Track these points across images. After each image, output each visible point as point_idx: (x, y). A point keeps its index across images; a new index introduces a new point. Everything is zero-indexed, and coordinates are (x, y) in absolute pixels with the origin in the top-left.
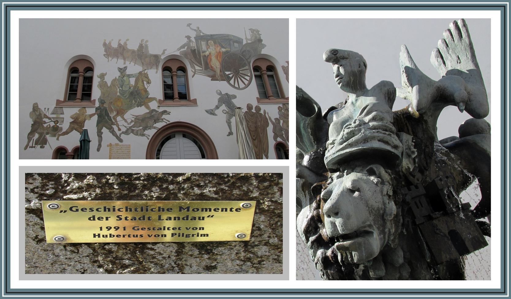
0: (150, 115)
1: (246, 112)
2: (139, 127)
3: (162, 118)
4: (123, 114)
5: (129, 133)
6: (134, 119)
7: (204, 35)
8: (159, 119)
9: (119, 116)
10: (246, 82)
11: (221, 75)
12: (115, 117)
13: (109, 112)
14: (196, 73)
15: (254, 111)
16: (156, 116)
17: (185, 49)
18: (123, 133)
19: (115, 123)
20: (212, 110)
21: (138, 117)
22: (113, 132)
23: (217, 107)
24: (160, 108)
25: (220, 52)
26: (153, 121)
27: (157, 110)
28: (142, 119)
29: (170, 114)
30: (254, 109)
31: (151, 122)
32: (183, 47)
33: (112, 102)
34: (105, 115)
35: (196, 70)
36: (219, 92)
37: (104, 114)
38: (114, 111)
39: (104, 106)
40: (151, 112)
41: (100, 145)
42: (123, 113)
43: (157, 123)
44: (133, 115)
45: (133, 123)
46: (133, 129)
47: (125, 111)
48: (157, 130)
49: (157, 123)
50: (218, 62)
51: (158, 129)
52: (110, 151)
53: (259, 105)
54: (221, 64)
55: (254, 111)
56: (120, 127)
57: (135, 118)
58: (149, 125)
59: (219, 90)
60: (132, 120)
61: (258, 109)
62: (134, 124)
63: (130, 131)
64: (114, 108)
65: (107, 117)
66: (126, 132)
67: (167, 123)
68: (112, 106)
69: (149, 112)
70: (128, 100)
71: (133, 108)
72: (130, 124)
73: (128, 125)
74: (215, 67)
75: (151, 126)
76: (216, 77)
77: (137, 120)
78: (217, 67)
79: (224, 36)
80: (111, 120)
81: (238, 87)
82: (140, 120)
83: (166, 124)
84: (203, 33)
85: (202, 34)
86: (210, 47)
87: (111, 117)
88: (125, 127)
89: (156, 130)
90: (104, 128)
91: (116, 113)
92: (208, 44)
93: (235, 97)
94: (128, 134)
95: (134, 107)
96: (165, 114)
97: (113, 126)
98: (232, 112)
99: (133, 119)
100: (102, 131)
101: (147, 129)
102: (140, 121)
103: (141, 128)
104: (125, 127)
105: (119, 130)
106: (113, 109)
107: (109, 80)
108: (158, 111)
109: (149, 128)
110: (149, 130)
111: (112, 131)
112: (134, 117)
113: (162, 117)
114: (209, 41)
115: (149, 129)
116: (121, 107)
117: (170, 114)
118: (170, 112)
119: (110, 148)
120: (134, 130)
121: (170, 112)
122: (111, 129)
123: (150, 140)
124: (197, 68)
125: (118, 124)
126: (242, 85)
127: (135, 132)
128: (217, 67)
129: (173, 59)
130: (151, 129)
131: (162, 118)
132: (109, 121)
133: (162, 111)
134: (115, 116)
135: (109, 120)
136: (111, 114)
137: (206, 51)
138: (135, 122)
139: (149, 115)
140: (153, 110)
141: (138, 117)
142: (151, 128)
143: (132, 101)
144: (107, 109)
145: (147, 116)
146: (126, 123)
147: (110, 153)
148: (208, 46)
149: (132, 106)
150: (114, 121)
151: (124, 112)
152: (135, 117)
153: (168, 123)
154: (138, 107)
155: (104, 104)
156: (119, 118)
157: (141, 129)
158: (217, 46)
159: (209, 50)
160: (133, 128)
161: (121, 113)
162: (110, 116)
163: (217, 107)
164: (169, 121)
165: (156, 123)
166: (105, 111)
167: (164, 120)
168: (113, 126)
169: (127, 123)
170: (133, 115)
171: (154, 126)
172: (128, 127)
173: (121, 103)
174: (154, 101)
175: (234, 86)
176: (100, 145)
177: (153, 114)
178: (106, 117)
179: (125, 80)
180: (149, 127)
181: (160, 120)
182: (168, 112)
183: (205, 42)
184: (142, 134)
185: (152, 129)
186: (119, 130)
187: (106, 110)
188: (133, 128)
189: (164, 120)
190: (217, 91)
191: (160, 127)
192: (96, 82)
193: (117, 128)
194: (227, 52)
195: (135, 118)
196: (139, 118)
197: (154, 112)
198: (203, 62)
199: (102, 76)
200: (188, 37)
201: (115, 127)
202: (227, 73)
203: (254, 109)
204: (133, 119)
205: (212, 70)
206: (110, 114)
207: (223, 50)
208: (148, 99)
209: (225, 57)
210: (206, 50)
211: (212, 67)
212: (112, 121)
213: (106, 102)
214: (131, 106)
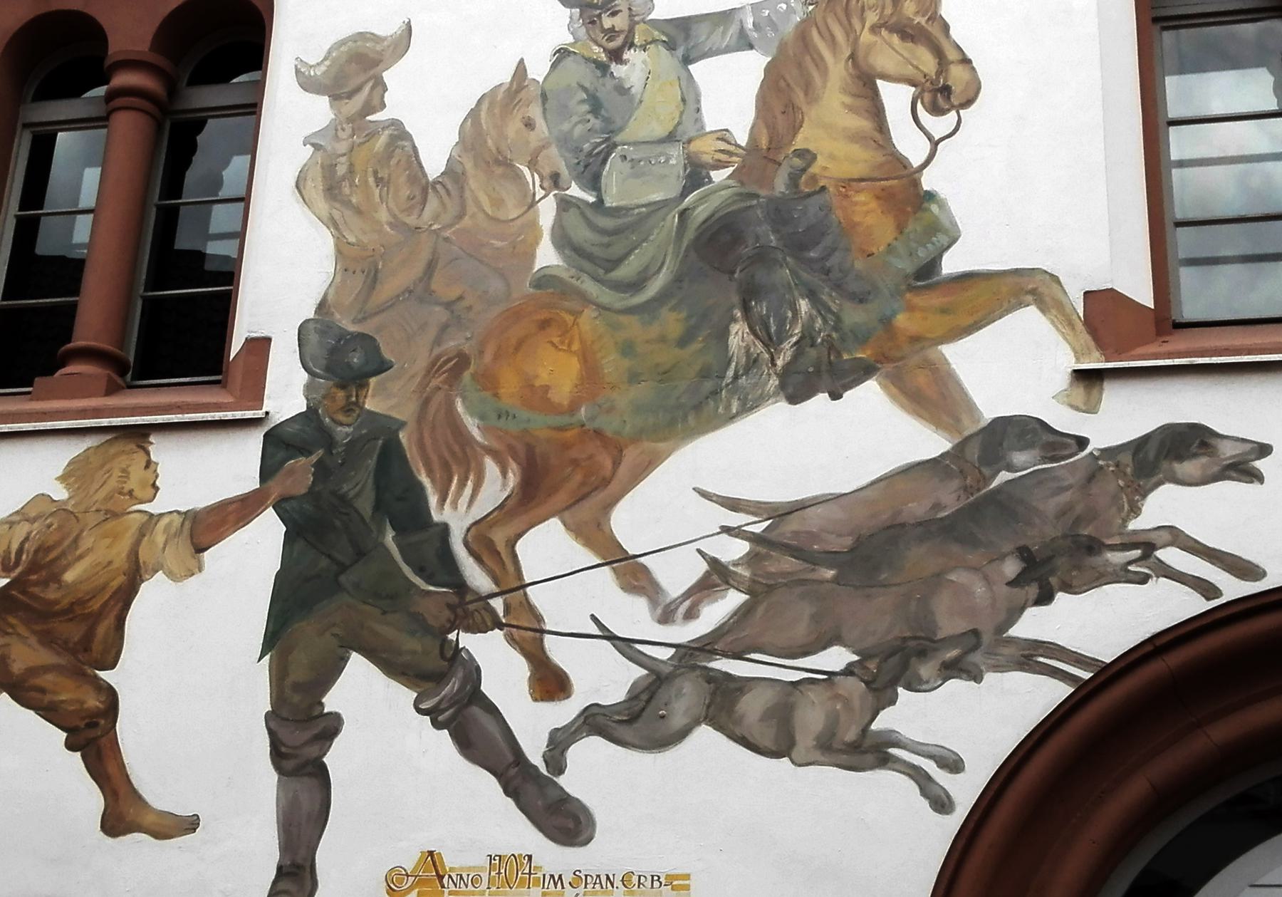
0: (967, 490)
2: (806, 654)
3: (1145, 521)
4: (600, 497)
5: (678, 721)
6: (740, 548)
8: (1094, 547)
9: (554, 524)
12: (499, 537)
16: (1052, 505)
19: (498, 604)
21: (793, 524)
24: (1114, 396)
26: (1011, 568)
27: (1064, 420)
28: (848, 541)
29: (1256, 477)
31: (980, 589)
33: (462, 361)
34: (378, 506)
37: (365, 505)
38: (491, 467)
39: (369, 405)
40: (973, 453)
42: (606, 482)
43: (1069, 588)
44: (733, 505)
45: (734, 599)
46: (728, 676)
47: (631, 456)
48: (1062, 691)
49: (1060, 597)
51: (1087, 675)
56: (557, 650)
57: (753, 538)
58: (949, 624)
60: (714, 563)
62: (742, 614)
64: (483, 430)
65: (400, 530)
66: (633, 719)
67: (1208, 589)
68: (460, 407)
69: (957, 453)
70: (672, 322)
71: (732, 418)
72: (691, 615)
73: (666, 618)
75: (975, 633)
77: (788, 564)
82: (830, 558)
83: (1191, 605)
87: (445, 529)
88: (625, 646)
89: (1051, 693)
90: (357, 666)
91: (513, 480)
95: (748, 407)
96: (1188, 468)
97: (468, 641)
99: (733, 551)
100: (331, 702)
101: (926, 670)
102: (830, 573)
103: (836, 658)
104: (625, 646)
106: (476, 434)
108: (1082, 442)
109: (953, 653)
110: (956, 686)
111: (453, 701)
112: (736, 519)
113: (1135, 511)
115: (953, 669)
116: (573, 408)
117: (1255, 477)
118: (1264, 450)
120: (744, 684)
121: (1264, 450)
122: (439, 678)
123: (954, 822)
125: (539, 619)
127: (752, 707)
130: (977, 678)
131: (1133, 525)
132: (417, 581)
133: (1146, 438)
134: (505, 512)
135: (420, 571)
136: (442, 500)
138: (758, 591)
139: (950, 499)
140: (1004, 426)
141: (793, 524)
142: (976, 657)
143: (723, 335)
144: (402, 436)
145: (917, 509)
146: (640, 605)
149: (715, 393)
150: (478, 578)
151: (616, 463)
152: (758, 528)
153: (1233, 588)
154: (794, 399)
155: (373, 381)
157: (831, 674)
162: (436, 517)
164: (1242, 569)
165: (1045, 598)
166: (372, 463)
167: (1171, 556)
168: (468, 641)
169: (654, 602)
171: (1015, 631)
172: (664, 654)
173: (574, 365)
174: (1028, 321)
177: (1004, 476)
178: (389, 537)
180: (951, 641)
181: (1117, 558)
182: (1228, 451)
184: (851, 735)
185: (990, 677)
187: (391, 455)
189: (1171, 556)
191: (1108, 653)
193: (521, 668)
195: (753, 538)
196: (813, 536)
197: (1019, 458)
204: (733, 551)
206: (433, 500)
208: (934, 300)
212: (460, 585)
213: (387, 354)
214: (708, 385)
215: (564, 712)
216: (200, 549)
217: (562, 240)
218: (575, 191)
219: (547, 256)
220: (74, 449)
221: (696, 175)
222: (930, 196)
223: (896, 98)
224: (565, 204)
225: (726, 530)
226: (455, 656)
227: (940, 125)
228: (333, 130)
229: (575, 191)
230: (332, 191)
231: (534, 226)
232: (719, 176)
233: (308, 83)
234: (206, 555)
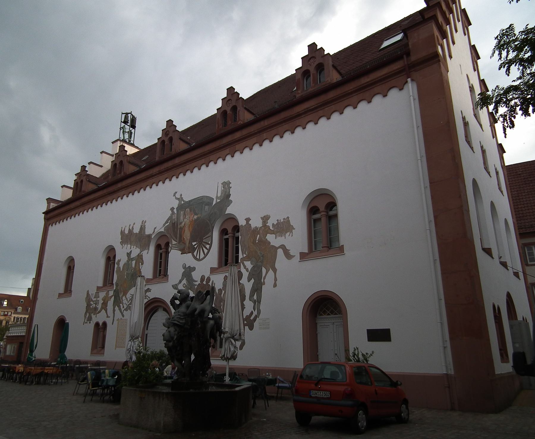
1: (199, 284)
7: (185, 202)
10: (206, 251)
11: (189, 248)
13: (120, 293)
14: (172, 248)
15: (204, 283)
17: (168, 224)
18: (125, 310)
20: (176, 284)
22: (120, 309)
23: (180, 282)
25: (192, 220)
29: (150, 292)
30: (205, 280)
32: (167, 222)
35: (173, 245)
36: (184, 265)
41: (113, 320)
44: (131, 295)
50: (189, 233)
52: (118, 324)
53: (209, 276)
54: (191, 234)
55: (204, 283)
59: (185, 264)
61: (209, 279)
63: (128, 308)
74: (186, 239)
76: (185, 250)
78: (187, 239)
79: (198, 200)
80: (120, 300)
81: (199, 258)
84: (184, 201)
85: (182, 202)
86: (186, 216)
92: (185, 214)
93: (194, 269)
94: (127, 311)
98: (189, 286)
105: (123, 307)
107: (121, 265)
112: (131, 296)
114: (187, 210)
117: (150, 292)
119: (118, 322)
124: (174, 242)
126: (202, 255)
128: (187, 239)
129: (161, 236)
137: (182, 222)
147: (118, 325)
148: (185, 216)
150: (121, 300)
153: (149, 299)
156: (124, 298)
158: (192, 214)
159: (185, 220)
160: (130, 305)
161: (125, 294)
163: (180, 282)
168: (121, 304)
170: (131, 295)
175: (195, 258)
176: (113, 320)
179: (130, 263)
183: (183, 212)
186: (123, 307)
188: (130, 305)
190: (183, 265)
192: (116, 266)
194: (198, 218)
198: (178, 236)
199: (119, 261)
200: (172, 209)
201: (121, 305)
202: (194, 244)
203: (205, 280)
205: (183, 243)
207: (195, 217)
209: (195, 226)
210: (182, 221)
211: (184, 239)
212: (120, 301)
215: (124, 309)
216: (111, 299)
217: (126, 276)
218: (127, 272)
219: (125, 277)
220: (106, 292)
221: (132, 271)
222: (141, 272)
223: (140, 264)
224: (127, 273)
225: (131, 296)
226: (120, 305)
227: (142, 266)
228: (117, 268)
229: (127, 272)
230: (117, 272)
231: (125, 274)
232: (133, 270)
233: (116, 264)
234: (111, 299)
